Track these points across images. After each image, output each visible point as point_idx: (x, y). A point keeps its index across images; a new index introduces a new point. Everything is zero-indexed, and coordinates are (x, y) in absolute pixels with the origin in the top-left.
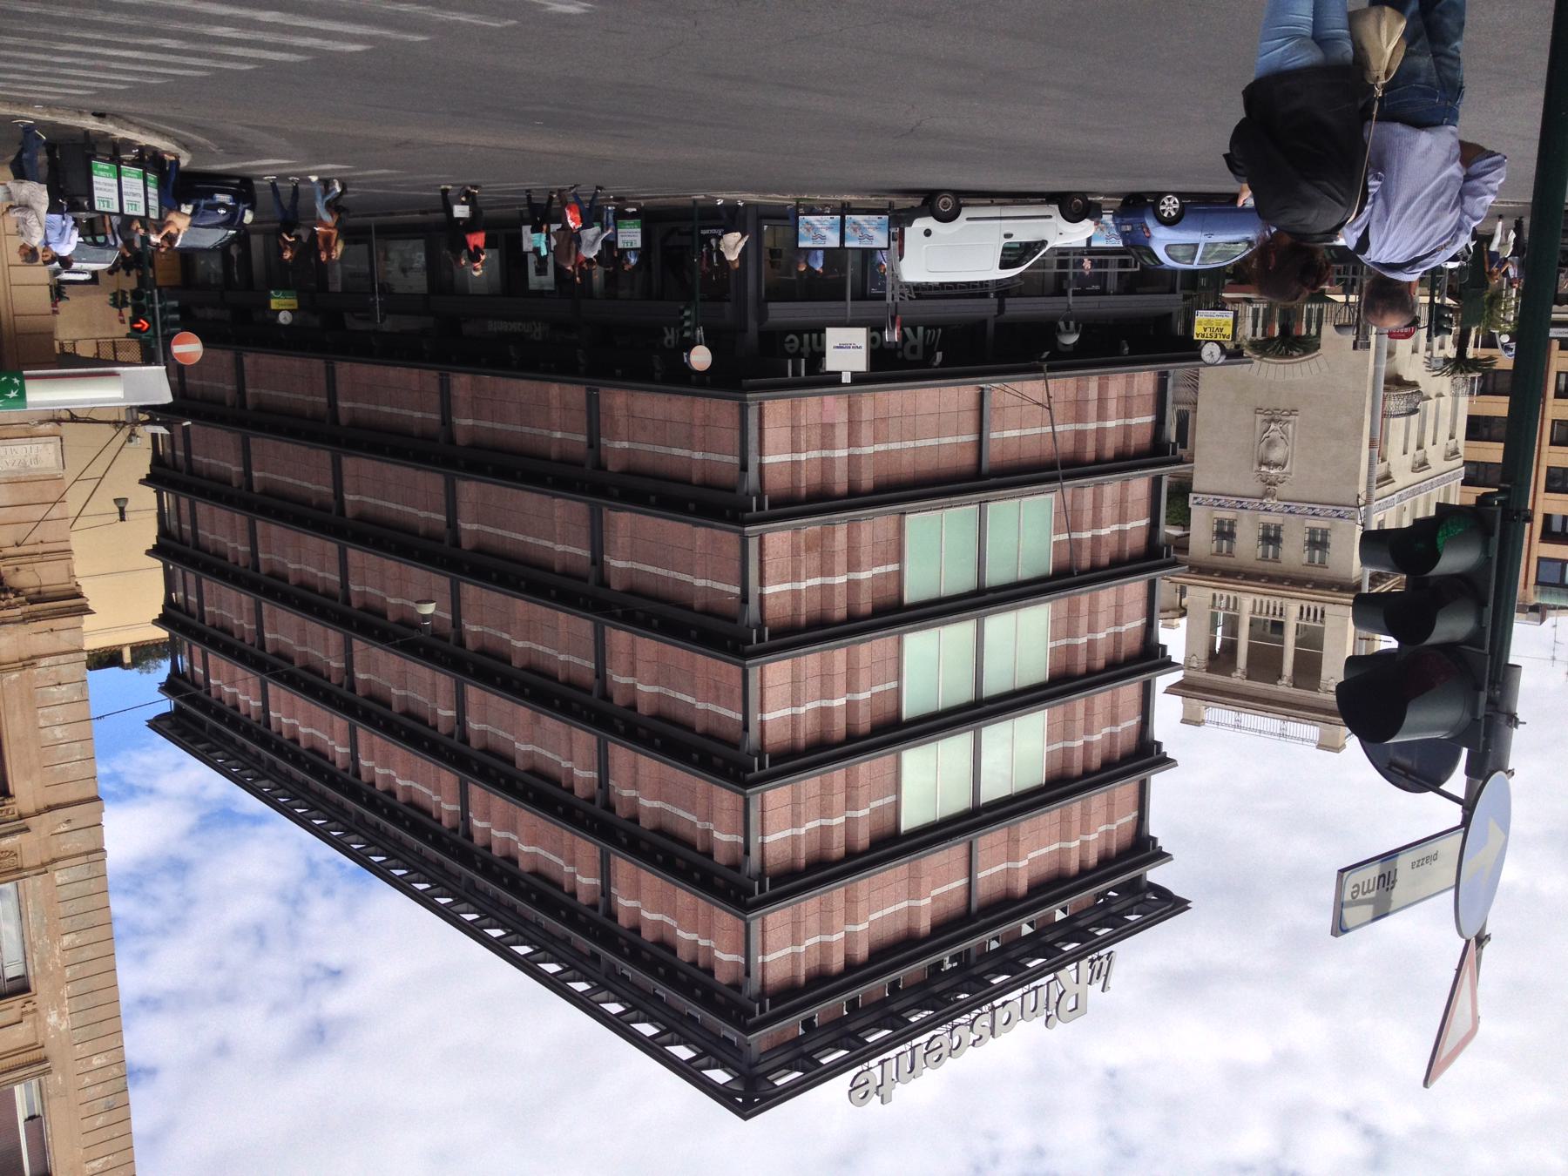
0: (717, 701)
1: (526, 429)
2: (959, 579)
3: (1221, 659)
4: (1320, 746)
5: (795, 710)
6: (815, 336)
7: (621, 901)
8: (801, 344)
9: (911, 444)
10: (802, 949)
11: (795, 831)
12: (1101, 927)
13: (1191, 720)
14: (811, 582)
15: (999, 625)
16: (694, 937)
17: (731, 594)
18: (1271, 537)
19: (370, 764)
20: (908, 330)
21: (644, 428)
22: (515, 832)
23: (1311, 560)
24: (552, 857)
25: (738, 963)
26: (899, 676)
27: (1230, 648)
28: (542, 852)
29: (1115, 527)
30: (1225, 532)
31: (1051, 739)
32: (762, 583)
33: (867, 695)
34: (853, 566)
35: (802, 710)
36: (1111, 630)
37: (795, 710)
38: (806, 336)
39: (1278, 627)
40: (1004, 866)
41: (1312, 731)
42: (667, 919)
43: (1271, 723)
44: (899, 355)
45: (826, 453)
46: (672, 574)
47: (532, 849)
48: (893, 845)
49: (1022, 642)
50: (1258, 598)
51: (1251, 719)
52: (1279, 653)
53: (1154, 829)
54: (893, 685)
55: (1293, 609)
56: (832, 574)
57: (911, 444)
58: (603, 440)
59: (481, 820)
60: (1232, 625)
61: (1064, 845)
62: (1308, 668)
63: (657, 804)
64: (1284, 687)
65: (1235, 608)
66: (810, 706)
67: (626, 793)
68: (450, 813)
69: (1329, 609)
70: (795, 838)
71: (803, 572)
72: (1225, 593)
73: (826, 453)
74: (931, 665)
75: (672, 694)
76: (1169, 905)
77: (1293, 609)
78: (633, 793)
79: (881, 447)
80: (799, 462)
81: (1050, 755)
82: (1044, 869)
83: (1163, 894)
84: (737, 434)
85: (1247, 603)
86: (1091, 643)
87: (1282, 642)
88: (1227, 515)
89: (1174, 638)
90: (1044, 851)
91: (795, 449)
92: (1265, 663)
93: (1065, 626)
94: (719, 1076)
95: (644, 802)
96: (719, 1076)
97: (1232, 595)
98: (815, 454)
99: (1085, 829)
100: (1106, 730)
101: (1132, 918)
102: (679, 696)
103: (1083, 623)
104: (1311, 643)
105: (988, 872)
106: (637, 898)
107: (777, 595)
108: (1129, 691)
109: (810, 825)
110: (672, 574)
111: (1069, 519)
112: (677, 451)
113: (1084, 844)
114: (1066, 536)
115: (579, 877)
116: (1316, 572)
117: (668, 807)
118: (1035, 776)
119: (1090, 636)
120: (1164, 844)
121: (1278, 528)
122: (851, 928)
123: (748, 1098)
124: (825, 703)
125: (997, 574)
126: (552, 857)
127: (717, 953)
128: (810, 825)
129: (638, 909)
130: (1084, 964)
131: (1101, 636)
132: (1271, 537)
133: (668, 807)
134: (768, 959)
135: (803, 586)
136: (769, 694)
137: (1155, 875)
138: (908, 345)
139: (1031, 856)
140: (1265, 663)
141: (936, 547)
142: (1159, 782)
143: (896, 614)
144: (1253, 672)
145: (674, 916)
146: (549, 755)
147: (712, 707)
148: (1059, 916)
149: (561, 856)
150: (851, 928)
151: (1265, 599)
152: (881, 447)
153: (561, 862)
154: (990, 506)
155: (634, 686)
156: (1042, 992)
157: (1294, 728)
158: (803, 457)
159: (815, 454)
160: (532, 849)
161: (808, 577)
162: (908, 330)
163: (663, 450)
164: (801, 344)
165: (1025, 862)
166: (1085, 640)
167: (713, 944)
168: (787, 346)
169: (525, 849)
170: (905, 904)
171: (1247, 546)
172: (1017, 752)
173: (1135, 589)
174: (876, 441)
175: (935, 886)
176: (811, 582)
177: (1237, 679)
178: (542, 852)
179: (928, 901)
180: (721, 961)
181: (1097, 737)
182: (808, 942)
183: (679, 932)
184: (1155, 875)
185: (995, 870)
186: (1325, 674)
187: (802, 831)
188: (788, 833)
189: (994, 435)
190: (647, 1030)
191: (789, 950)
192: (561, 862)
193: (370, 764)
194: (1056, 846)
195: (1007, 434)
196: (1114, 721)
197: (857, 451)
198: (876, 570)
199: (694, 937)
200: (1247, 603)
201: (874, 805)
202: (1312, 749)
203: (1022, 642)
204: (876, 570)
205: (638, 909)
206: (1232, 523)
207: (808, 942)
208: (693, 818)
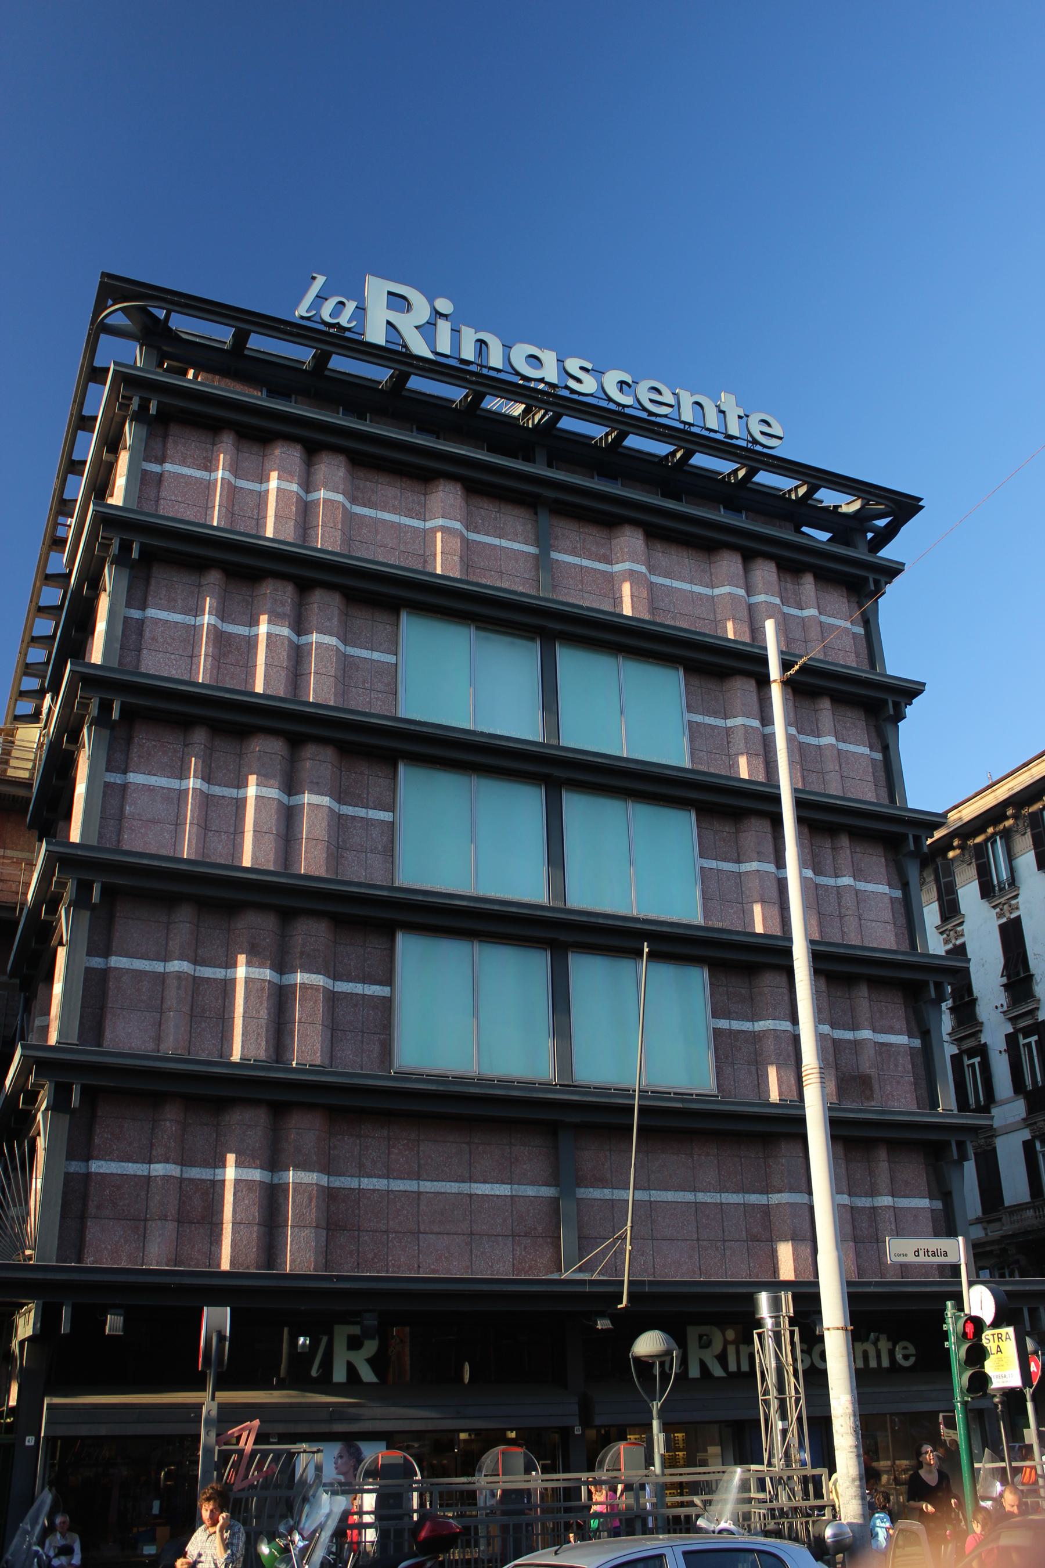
6: (873, 1364)
9: (702, 1197)
38: (886, 1363)
44: (730, 1335)
57: (702, 1197)
71: (870, 1052)
82: (388, 489)
107: (891, 1031)
135: (866, 1034)
136: (887, 915)
138: (717, 1346)
152: (754, 1199)
158: (886, 1201)
162: (718, 1372)
164: (892, 1354)
166: (307, 798)
168: (912, 1350)
185: (496, 541)
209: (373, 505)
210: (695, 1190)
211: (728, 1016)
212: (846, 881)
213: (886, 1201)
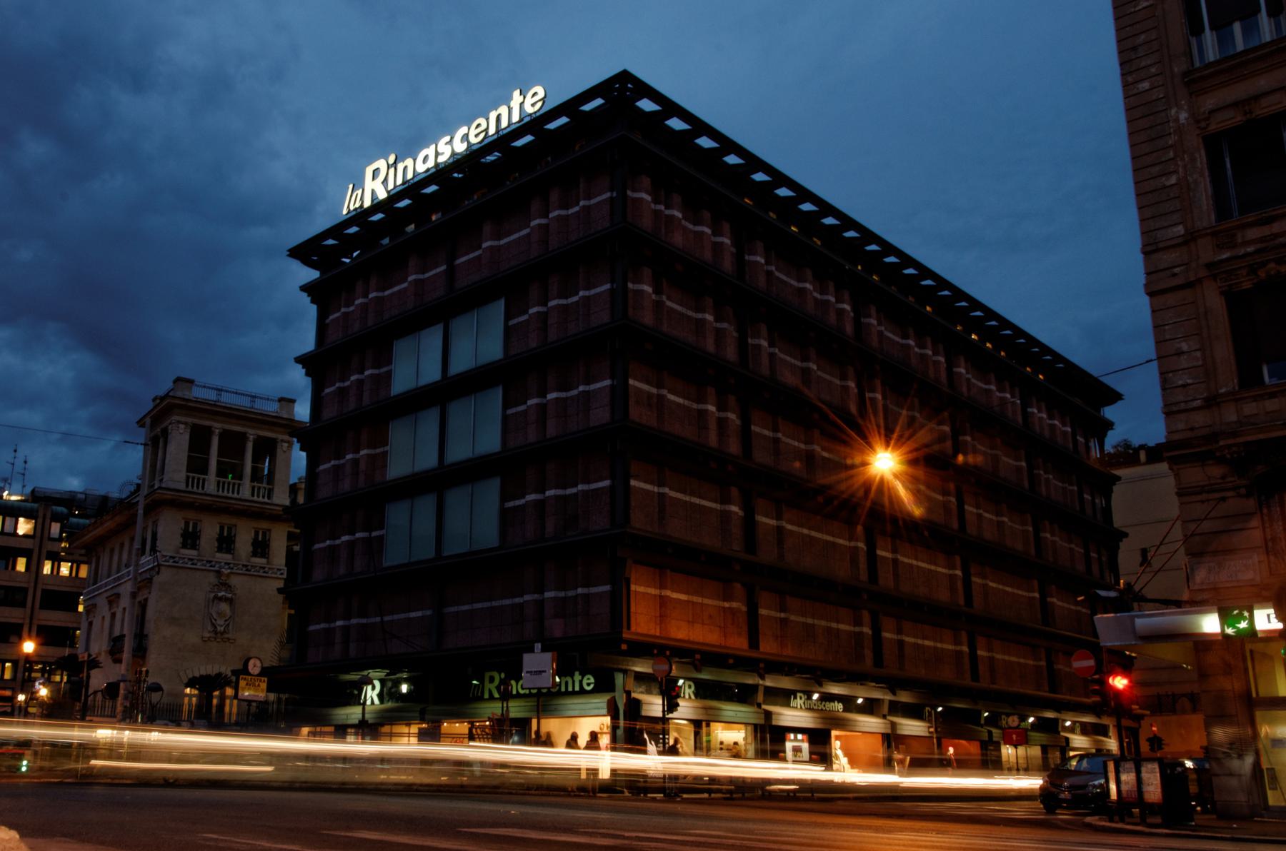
0: (650, 395)
1: (810, 621)
2: (456, 499)
3: (266, 449)
4: (191, 382)
5: (587, 388)
6: (570, 689)
7: (727, 241)
8: (581, 682)
9: (495, 604)
10: (582, 203)
11: (587, 293)
12: (356, 233)
13: (288, 402)
14: (574, 490)
15: (428, 460)
16: (668, 212)
17: (637, 478)
18: (226, 543)
19: (935, 358)
20: (497, 695)
21: (710, 617)
22: (815, 299)
23: (195, 525)
24: (784, 277)
25: (634, 190)
26: (505, 419)
27: (257, 458)
28: (793, 282)
29: (338, 542)
30: (261, 547)
31: (389, 375)
32: (612, 487)
33: (530, 402)
34: (540, 505)
35: (581, 388)
36: (342, 461)
37: (587, 388)
38: (577, 688)
39: (221, 473)
40: (427, 275)
41: (198, 393)
42: (691, 227)
43: (227, 399)
45: (562, 594)
46: (687, 498)
47: (801, 285)
48: (511, 286)
49: (411, 450)
50: (235, 495)
51: (244, 403)
52: (219, 455)
53: (313, 309)
54: (509, 412)
55: (211, 487)
56: (556, 497)
57: (495, 604)
58: (744, 609)
59: (844, 310)
60: (256, 476)
61: (380, 294)
62: (199, 439)
63: (700, 316)
64: (218, 426)
65: (253, 488)
66: (575, 392)
67: (725, 325)
68: (869, 316)
69: (182, 486)
70: (588, 288)
72: (261, 499)
73: (562, 594)
74: (480, 430)
75: (687, 403)
76: (304, 252)
77: (211, 487)
78: (718, 325)
79: (517, 600)
80: (582, 586)
81: (390, 362)
83: (307, 262)
84: (633, 609)
85: (246, 492)
86: (357, 451)
87: (218, 462)
88: (260, 561)
89: (298, 460)
90: (396, 289)
91: (587, 596)
92: (233, 445)
93: (379, 462)
94: (646, 105)
95: (709, 317)
96: (646, 105)
97: (255, 498)
98: (571, 593)
99: (364, 307)
100: (347, 383)
101: (331, 242)
102: (680, 401)
103: (362, 466)
104: (197, 465)
105: (438, 270)
106: (715, 244)
107: (601, 479)
108: (328, 413)
109: (575, 299)
110: (687, 498)
111: (375, 548)
112: (683, 597)
113: (366, 296)
114: (374, 534)
115: (763, 261)
116: (191, 515)
117: (690, 313)
118: (402, 349)
119: (357, 456)
120: (305, 298)
121: (220, 550)
122: (543, 221)
123: (623, 88)
124: (563, 395)
125: (426, 506)
126: (784, 277)
127: (648, 198)
128: (575, 299)
129: (714, 234)
130: (367, 203)
131: (349, 457)
132: (226, 543)
133: (690, 313)
134: (608, 195)
135: (580, 487)
137: (312, 275)
139: (405, 285)
140: (233, 445)
141: (476, 520)
142: (308, 343)
143: (505, 467)
144: (243, 437)
145: (685, 228)
146: (788, 358)
147: (654, 391)
148: (386, 241)
149: (778, 278)
150: (543, 221)
151: (225, 494)
152: (517, 600)
153: (777, 274)
154: (432, 554)
155: (719, 410)
156: (399, 181)
157: (211, 396)
158: (580, 590)
159: (571, 593)
160: (801, 285)
161: (576, 495)
163: (696, 599)
164: (581, 682)
165: (410, 279)
166: (363, 452)
167: (653, 206)
168: (592, 680)
169: (808, 286)
170: (502, 242)
171: (244, 541)
172: (416, 364)
173: (324, 492)
174: (521, 605)
175: (479, 257)
176: (574, 490)
177: (252, 433)
178: (793, 282)
179: (485, 245)
180: (647, 192)
181: (353, 378)
182: (576, 209)
183: (678, 214)
184: (312, 275)
186: (187, 437)
187: (581, 293)
188: (593, 292)
189: (429, 613)
190: (705, 142)
191: (593, 202)
192: (777, 274)
193: (935, 358)
194: (387, 293)
195: (419, 614)
196: (342, 392)
197: (536, 596)
198: (522, 502)
199: (668, 212)
200: (246, 492)
201: (525, 317)
202: (199, 380)
203: (411, 450)
204: (522, 502)
205: (714, 234)
206: (255, 554)
207: (576, 209)
208: (669, 303)
209: (391, 287)
210: (491, 600)
211: (514, 499)
212: (581, 388)
213: (580, 590)
